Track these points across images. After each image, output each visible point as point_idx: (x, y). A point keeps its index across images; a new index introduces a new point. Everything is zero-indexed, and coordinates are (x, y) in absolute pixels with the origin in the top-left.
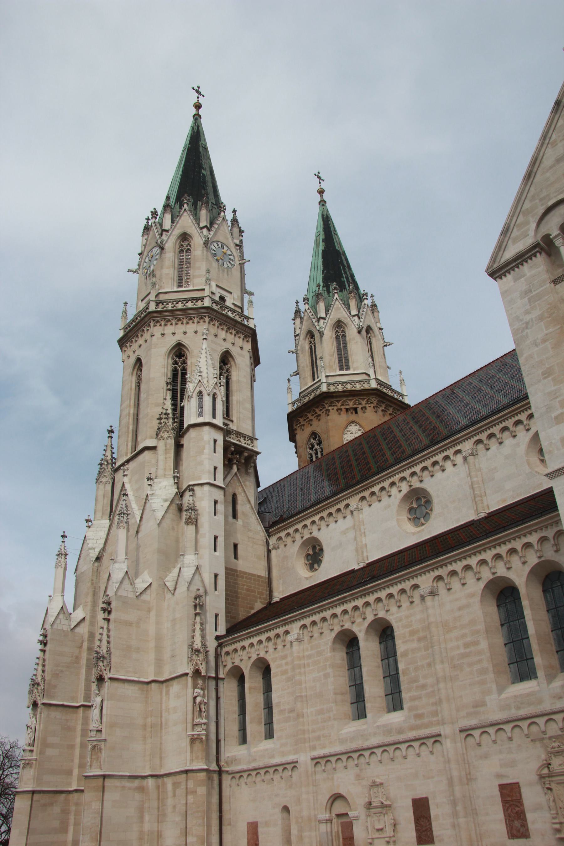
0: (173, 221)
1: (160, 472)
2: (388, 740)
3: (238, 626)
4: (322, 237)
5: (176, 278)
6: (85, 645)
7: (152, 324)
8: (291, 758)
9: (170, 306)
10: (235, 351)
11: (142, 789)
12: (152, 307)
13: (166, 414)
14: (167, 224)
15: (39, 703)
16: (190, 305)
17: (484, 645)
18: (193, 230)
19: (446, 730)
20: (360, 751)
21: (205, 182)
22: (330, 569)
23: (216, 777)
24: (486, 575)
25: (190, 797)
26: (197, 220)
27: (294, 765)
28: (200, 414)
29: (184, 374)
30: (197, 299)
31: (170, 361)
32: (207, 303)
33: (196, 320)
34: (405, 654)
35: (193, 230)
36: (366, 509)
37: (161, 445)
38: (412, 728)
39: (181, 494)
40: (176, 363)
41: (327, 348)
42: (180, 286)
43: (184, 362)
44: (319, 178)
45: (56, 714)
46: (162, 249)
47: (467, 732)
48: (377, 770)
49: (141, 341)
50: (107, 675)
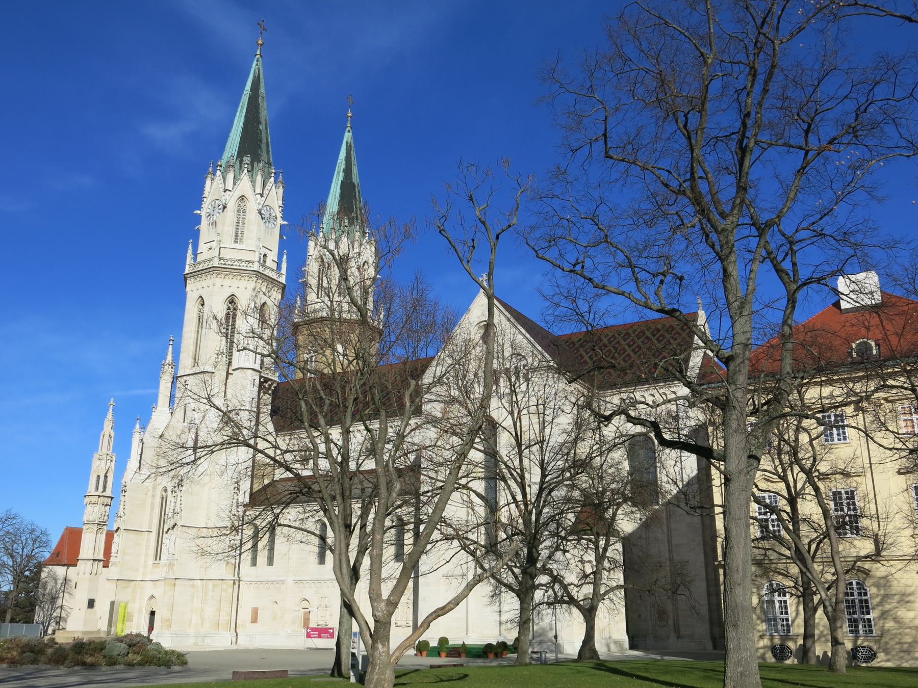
0: (234, 184)
3: (256, 499)
4: (343, 167)
5: (234, 234)
6: (150, 493)
7: (215, 275)
8: (282, 579)
9: (229, 262)
11: (193, 586)
12: (216, 263)
13: (223, 353)
14: (229, 185)
15: (122, 528)
16: (243, 266)
18: (249, 194)
21: (261, 140)
23: (237, 582)
25: (224, 594)
26: (254, 186)
27: (283, 582)
30: (249, 262)
31: (226, 307)
32: (256, 267)
33: (247, 278)
35: (249, 194)
37: (217, 373)
40: (229, 308)
42: (236, 242)
45: (131, 535)
46: (225, 207)
49: (204, 284)
50: (179, 523)
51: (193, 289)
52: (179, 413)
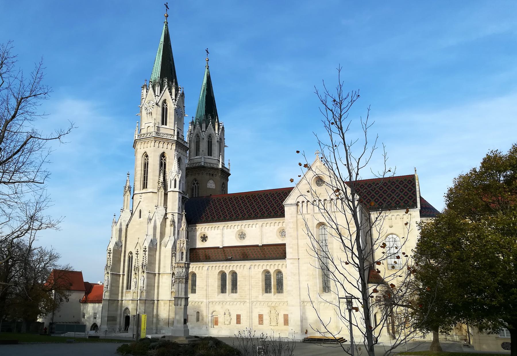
1: (159, 204)
2: (232, 300)
10: (182, 157)
17: (261, 284)
19: (248, 301)
20: (223, 302)
22: (208, 244)
24: (264, 268)
28: (175, 187)
29: (165, 165)
30: (172, 135)
34: (240, 281)
36: (225, 230)
37: (160, 193)
38: (239, 299)
39: (166, 214)
41: (204, 146)
43: (165, 160)
44: (207, 52)
47: (253, 302)
48: (227, 307)
51: (141, 149)
52: (137, 214)
